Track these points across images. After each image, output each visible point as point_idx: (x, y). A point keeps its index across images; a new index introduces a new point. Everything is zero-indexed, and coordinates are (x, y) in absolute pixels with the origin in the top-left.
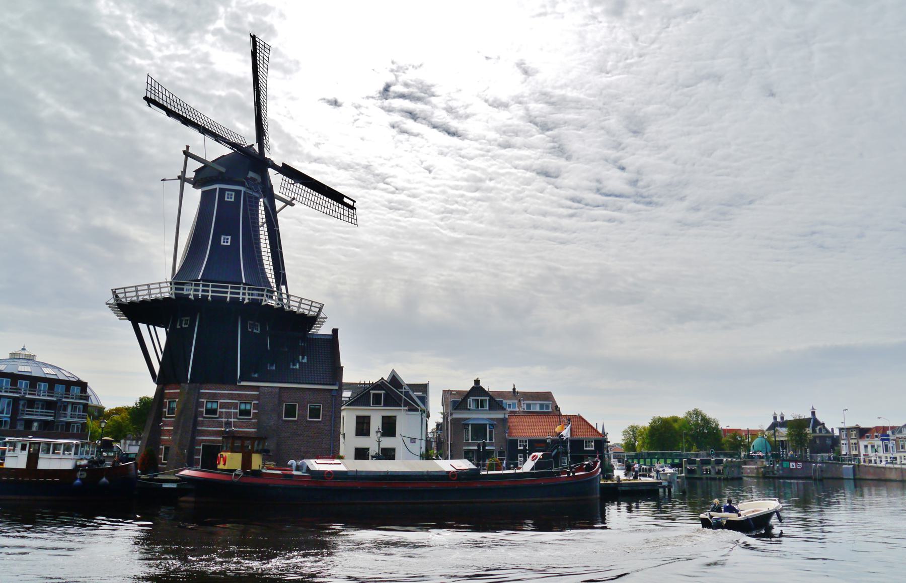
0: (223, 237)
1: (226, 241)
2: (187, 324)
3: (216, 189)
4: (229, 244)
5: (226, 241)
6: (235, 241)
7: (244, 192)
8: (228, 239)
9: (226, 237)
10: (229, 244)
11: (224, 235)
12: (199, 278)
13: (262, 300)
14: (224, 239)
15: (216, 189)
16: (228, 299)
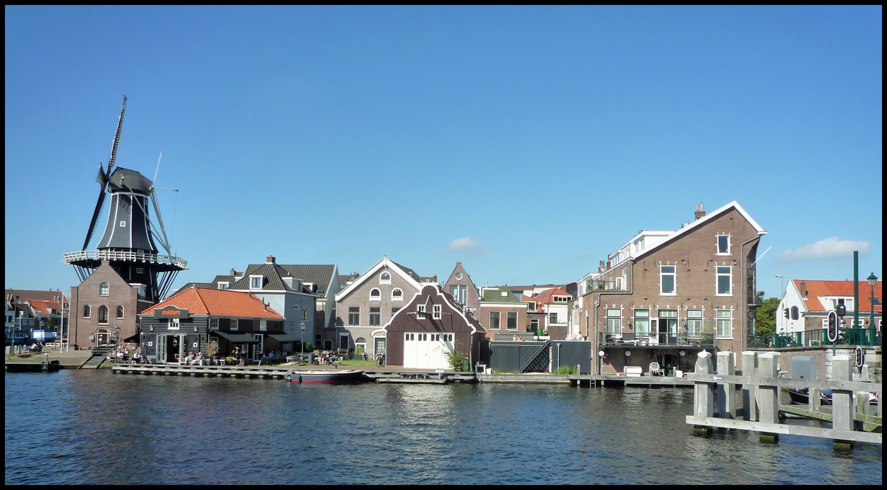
1: (123, 224)
6: (127, 224)
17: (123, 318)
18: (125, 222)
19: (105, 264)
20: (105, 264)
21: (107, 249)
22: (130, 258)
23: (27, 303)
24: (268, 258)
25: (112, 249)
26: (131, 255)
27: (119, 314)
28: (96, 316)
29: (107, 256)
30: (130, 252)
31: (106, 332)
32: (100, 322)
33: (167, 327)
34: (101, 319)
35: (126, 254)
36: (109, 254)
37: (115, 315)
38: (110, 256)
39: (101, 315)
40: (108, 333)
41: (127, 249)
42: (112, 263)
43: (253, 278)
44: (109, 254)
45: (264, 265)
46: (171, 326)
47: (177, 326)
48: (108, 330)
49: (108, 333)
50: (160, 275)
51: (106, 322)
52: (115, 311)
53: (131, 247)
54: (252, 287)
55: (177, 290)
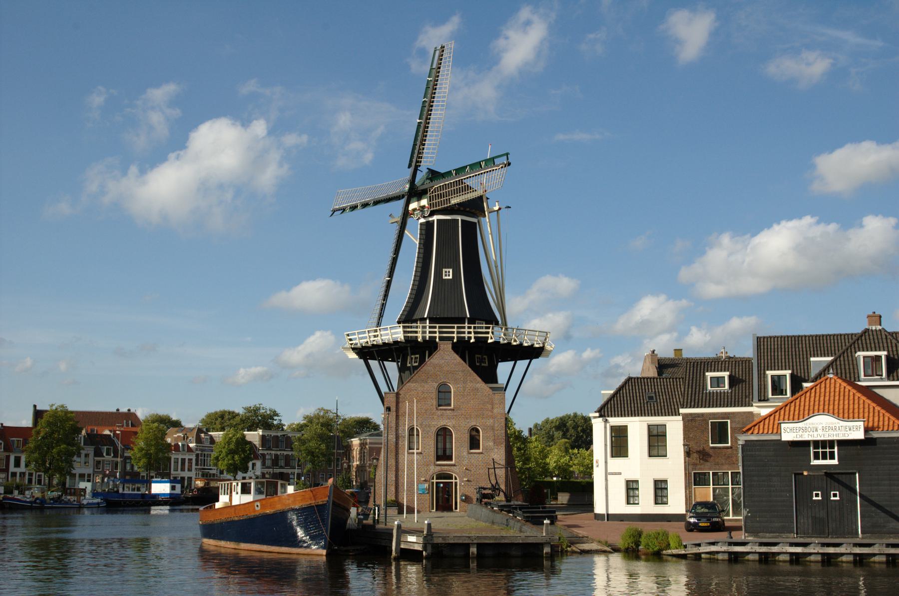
0: (444, 270)
1: (448, 274)
2: (417, 363)
3: (433, 221)
4: (451, 277)
5: (448, 274)
6: (456, 274)
7: (462, 220)
8: (449, 272)
9: (447, 270)
10: (451, 277)
11: (445, 268)
12: (426, 316)
13: (488, 337)
14: (446, 272)
15: (433, 221)
16: (455, 340)
17: (481, 451)
18: (451, 271)
19: (446, 348)
20: (446, 348)
21: (423, 320)
22: (466, 335)
23: (107, 432)
24: (868, 316)
25: (433, 320)
26: (466, 330)
27: (474, 443)
28: (431, 451)
29: (424, 332)
30: (466, 325)
31: (450, 477)
32: (439, 458)
33: (811, 462)
34: (440, 453)
35: (475, 328)
36: (428, 330)
37: (467, 444)
38: (430, 332)
39: (441, 445)
40: (454, 481)
41: (461, 320)
42: (461, 347)
43: (864, 357)
44: (428, 330)
45: (866, 331)
46: (817, 457)
47: (832, 457)
48: (454, 475)
49: (454, 481)
50: (503, 369)
51: (450, 458)
52: (467, 437)
53: (468, 316)
54: (865, 376)
55: (612, 392)
